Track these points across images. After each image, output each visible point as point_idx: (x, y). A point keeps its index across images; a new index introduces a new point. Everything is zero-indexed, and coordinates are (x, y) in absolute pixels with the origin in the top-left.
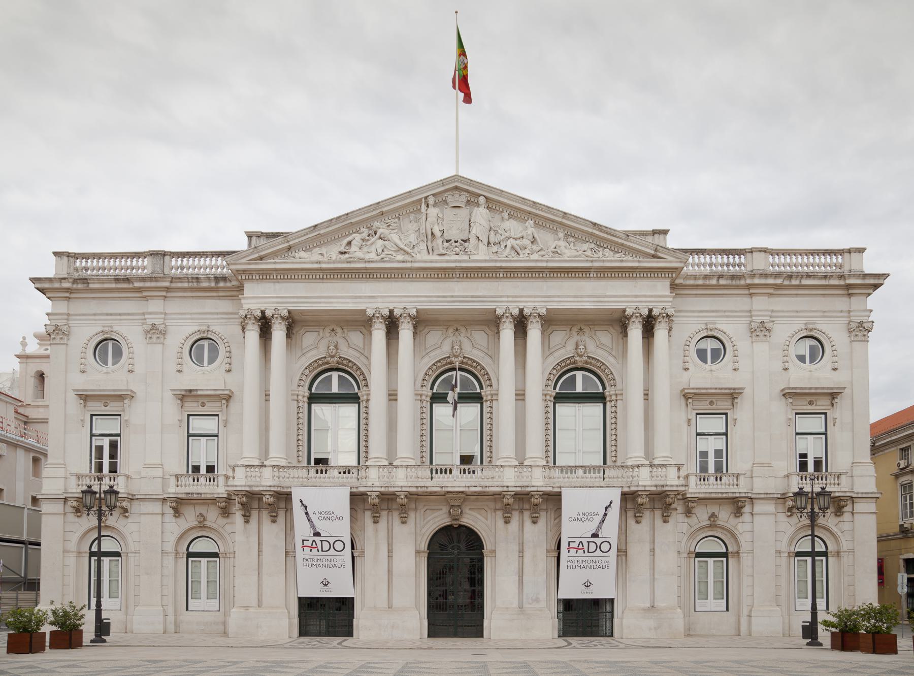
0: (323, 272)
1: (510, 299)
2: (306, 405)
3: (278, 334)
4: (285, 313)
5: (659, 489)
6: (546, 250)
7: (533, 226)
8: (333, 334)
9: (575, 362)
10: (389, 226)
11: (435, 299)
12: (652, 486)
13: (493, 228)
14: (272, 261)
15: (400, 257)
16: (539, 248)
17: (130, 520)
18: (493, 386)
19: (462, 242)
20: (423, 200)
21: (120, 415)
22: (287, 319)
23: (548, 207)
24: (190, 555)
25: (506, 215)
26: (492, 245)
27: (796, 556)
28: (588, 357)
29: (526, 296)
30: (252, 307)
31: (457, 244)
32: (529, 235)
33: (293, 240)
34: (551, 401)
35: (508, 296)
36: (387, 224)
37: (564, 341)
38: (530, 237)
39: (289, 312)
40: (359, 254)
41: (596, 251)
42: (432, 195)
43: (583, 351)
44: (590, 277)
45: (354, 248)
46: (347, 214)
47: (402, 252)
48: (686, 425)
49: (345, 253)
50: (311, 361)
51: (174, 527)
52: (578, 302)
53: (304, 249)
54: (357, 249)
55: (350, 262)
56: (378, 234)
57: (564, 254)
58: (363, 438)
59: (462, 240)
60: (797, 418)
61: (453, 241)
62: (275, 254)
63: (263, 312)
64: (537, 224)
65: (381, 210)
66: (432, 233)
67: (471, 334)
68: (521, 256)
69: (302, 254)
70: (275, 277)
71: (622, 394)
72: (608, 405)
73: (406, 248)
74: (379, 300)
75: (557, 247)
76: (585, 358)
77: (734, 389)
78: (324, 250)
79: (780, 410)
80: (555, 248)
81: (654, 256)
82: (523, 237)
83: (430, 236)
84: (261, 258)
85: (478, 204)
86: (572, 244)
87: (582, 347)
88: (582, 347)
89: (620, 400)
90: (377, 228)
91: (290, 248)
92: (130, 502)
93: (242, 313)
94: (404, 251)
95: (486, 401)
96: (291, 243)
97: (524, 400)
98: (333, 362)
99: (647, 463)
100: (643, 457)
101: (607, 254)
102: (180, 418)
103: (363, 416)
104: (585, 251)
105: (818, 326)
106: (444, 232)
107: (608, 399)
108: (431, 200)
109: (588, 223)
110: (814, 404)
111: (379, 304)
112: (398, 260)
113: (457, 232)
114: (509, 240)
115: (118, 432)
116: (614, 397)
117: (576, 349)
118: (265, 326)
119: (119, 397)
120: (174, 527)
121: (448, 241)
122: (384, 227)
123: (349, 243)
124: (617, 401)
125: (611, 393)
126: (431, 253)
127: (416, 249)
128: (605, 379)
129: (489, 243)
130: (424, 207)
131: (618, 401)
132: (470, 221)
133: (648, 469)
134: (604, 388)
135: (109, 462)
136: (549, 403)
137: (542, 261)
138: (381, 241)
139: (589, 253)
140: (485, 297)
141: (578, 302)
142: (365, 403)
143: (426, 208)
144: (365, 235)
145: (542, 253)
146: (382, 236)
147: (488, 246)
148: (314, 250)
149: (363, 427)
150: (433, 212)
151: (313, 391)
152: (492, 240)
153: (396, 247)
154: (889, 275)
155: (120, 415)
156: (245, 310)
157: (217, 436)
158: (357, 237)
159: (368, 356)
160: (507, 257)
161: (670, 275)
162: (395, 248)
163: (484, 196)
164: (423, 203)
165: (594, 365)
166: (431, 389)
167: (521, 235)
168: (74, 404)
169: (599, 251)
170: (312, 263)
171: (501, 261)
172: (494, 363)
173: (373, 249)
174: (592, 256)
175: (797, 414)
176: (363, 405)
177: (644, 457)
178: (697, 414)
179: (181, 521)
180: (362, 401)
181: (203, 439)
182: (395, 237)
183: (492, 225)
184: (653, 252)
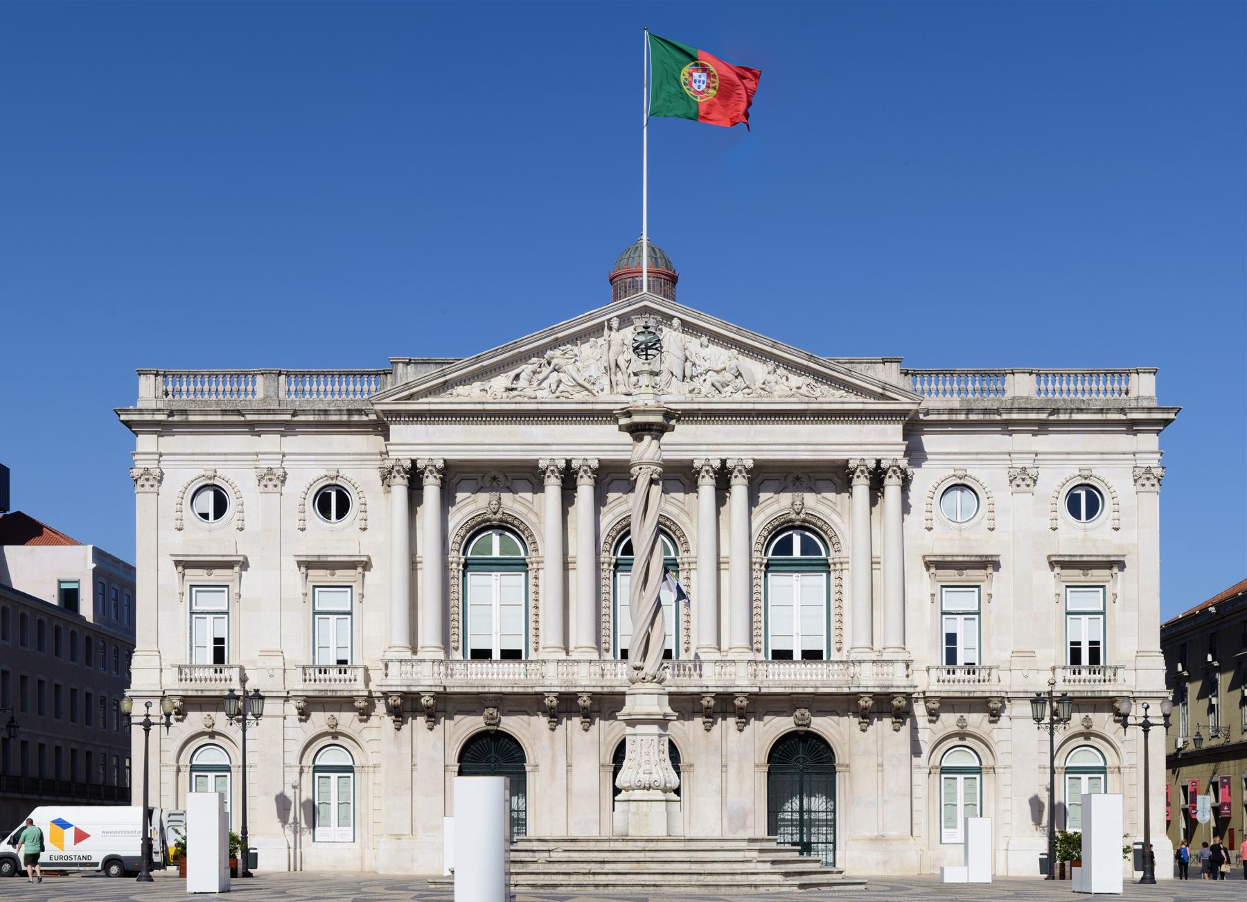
1: (711, 447)
4: (440, 464)
8: (495, 484)
9: (791, 521)
10: (564, 354)
11: (620, 448)
13: (689, 358)
15: (579, 396)
16: (744, 385)
18: (691, 550)
21: (227, 586)
26: (689, 380)
28: (807, 513)
32: (733, 369)
33: (450, 373)
34: (761, 571)
35: (708, 444)
39: (445, 461)
40: (529, 392)
43: (800, 507)
45: (522, 383)
47: (579, 388)
49: (512, 389)
50: (467, 519)
55: (520, 403)
56: (552, 365)
57: (775, 391)
58: (532, 618)
66: (617, 365)
69: (460, 390)
73: (585, 384)
74: (554, 448)
75: (766, 382)
76: (802, 516)
77: (987, 556)
78: (487, 385)
79: (1049, 581)
80: (764, 383)
82: (725, 369)
84: (410, 397)
86: (785, 378)
89: (845, 569)
90: (551, 358)
91: (445, 382)
94: (584, 387)
95: (683, 570)
96: (448, 377)
98: (495, 520)
102: (304, 592)
103: (532, 589)
105: (1094, 473)
107: (832, 567)
111: (554, 453)
112: (577, 400)
115: (225, 608)
116: (838, 566)
117: (792, 505)
118: (415, 478)
119: (229, 565)
123: (517, 377)
125: (835, 560)
129: (684, 376)
131: (844, 571)
135: (214, 647)
139: (804, 390)
140: (681, 444)
144: (536, 366)
145: (747, 390)
146: (557, 367)
147: (683, 381)
149: (532, 604)
151: (469, 555)
153: (571, 380)
155: (227, 586)
157: (350, 613)
159: (538, 512)
162: (572, 383)
165: (815, 525)
166: (614, 555)
168: (170, 573)
171: (699, 403)
172: (692, 522)
176: (532, 574)
180: (531, 570)
181: (333, 618)
182: (571, 368)
183: (688, 355)
184: (880, 391)
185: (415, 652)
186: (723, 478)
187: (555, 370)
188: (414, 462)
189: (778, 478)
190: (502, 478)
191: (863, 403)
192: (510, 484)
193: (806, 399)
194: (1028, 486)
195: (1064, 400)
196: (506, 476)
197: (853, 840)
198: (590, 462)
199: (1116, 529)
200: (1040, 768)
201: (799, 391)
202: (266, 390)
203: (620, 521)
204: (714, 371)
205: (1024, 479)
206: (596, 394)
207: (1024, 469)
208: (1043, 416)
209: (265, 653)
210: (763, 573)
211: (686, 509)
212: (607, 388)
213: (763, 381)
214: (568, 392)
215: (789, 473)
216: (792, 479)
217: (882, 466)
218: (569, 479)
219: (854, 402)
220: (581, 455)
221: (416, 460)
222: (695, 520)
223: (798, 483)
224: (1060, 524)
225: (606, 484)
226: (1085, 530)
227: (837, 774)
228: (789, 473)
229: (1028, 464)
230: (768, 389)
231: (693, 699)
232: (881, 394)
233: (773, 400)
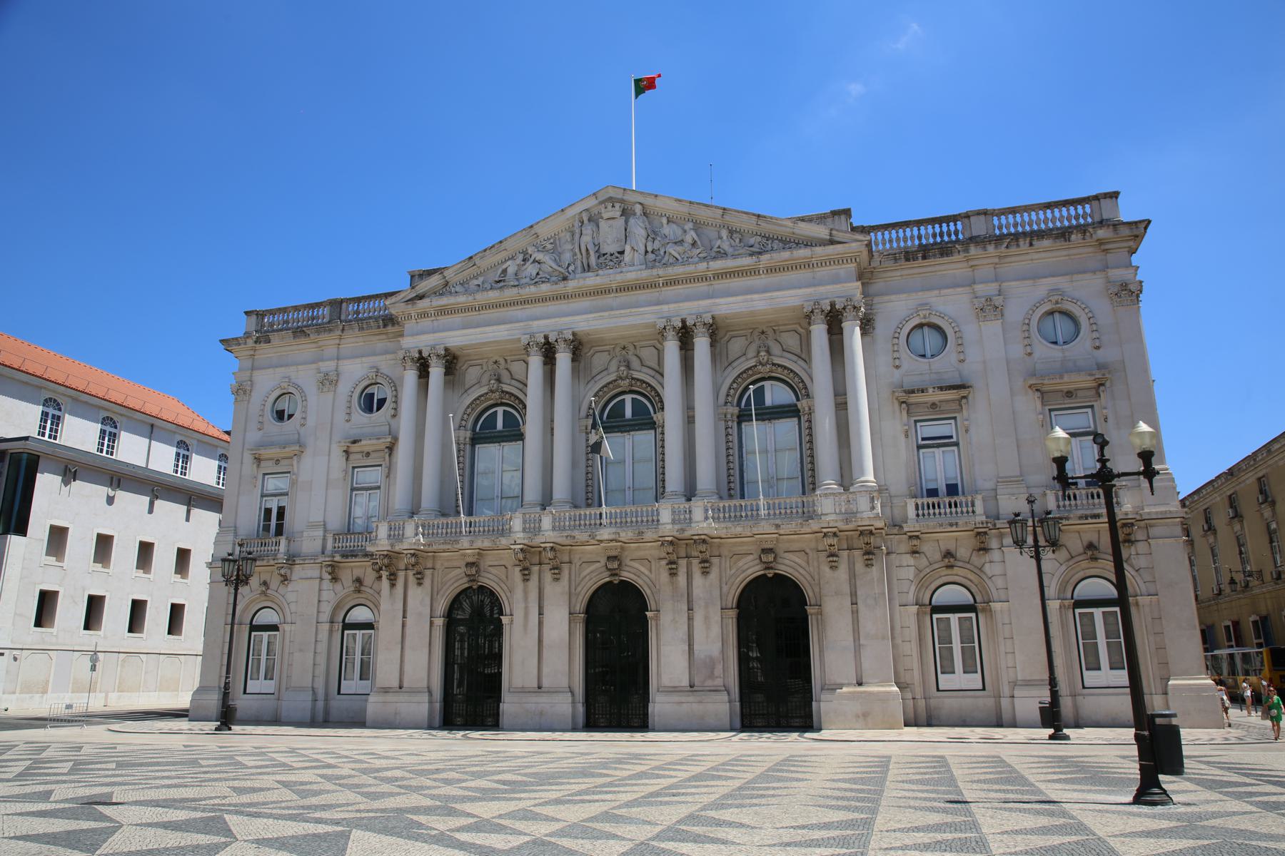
2: (468, 447)
3: (436, 372)
17: (290, 588)
22: (445, 356)
24: (347, 626)
25: (664, 220)
31: (614, 256)
34: (733, 421)
48: (903, 436)
49: (500, 281)
51: (331, 594)
56: (533, 258)
59: (619, 253)
63: (420, 352)
66: (587, 250)
81: (832, 242)
86: (737, 240)
87: (763, 354)
88: (763, 354)
92: (290, 568)
93: (401, 354)
120: (331, 594)
121: (604, 255)
123: (505, 271)
127: (571, 268)
129: (646, 252)
132: (626, 230)
136: (730, 423)
152: (649, 249)
154: (1149, 222)
163: (640, 203)
167: (680, 239)
178: (916, 422)
179: (338, 587)
186: (685, 336)
196: (506, 360)
197: (828, 689)
199: (1098, 348)
201: (751, 249)
202: (331, 315)
205: (990, 308)
207: (989, 299)
209: (312, 526)
210: (735, 424)
211: (661, 371)
212: (579, 269)
213: (717, 246)
215: (754, 329)
216: (757, 334)
217: (837, 307)
218: (549, 353)
223: (763, 336)
227: (809, 617)
230: (722, 251)
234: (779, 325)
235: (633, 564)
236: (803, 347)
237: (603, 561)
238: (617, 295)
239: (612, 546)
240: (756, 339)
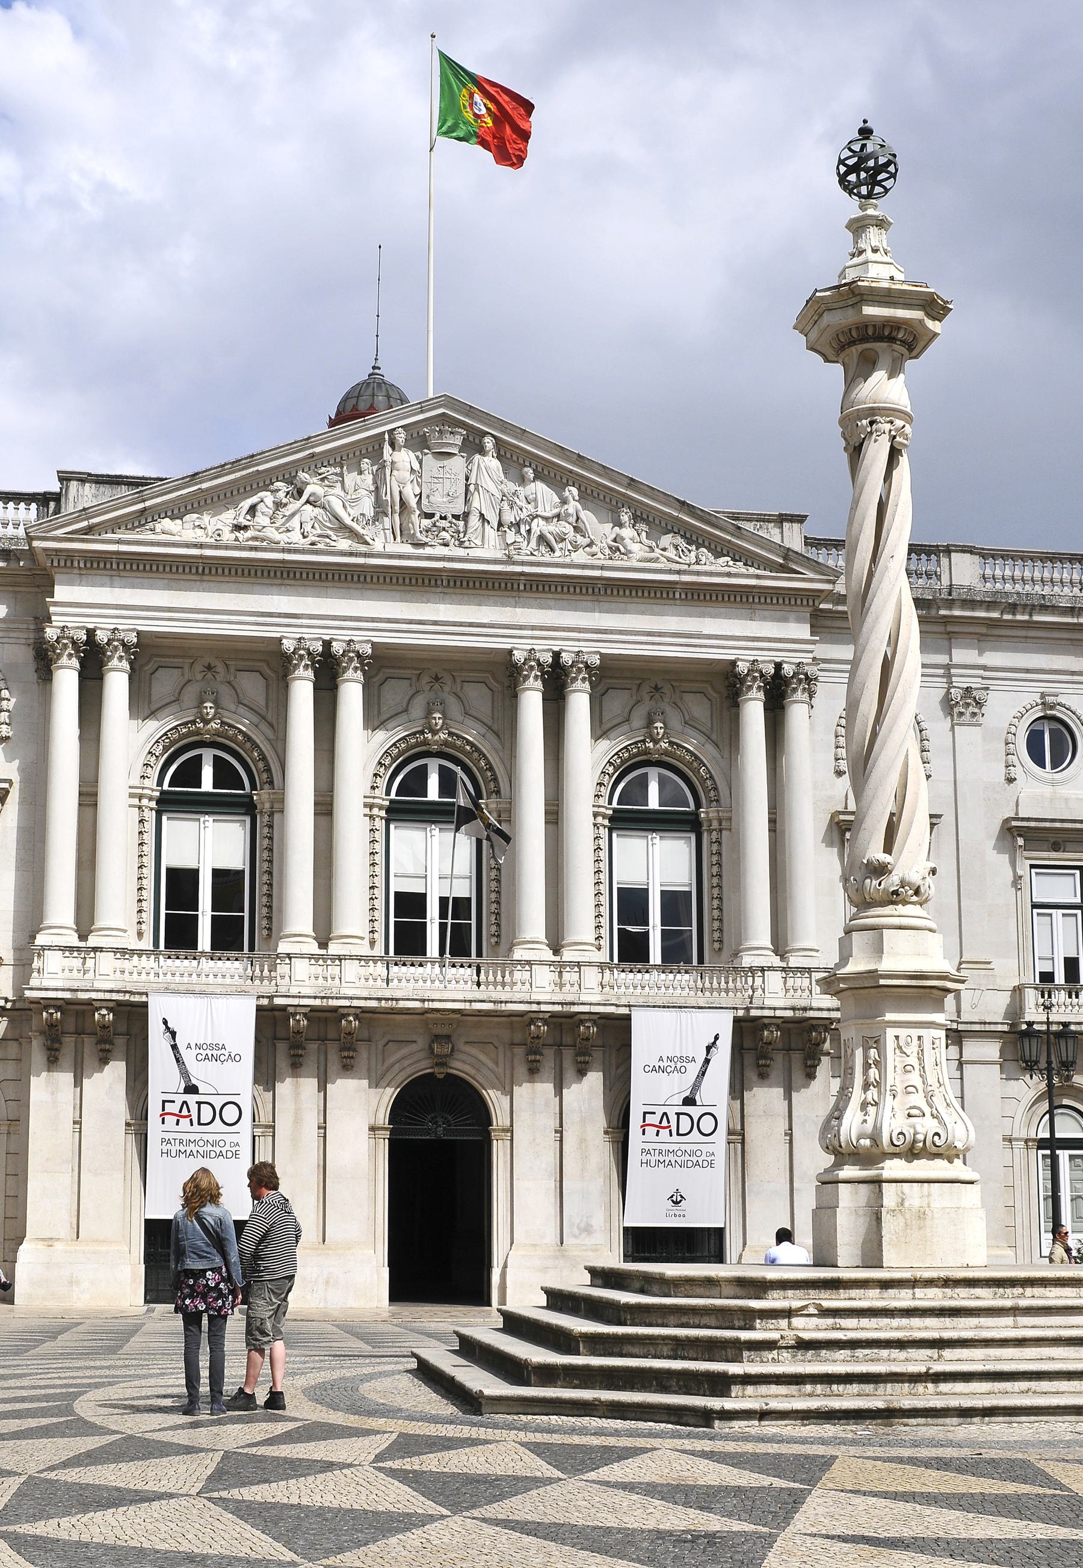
0: (204, 561)
5: (799, 1014)
6: (600, 544)
7: (577, 498)
10: (322, 480)
12: (785, 1009)
14: (110, 536)
15: (344, 544)
16: (587, 541)
19: (454, 520)
20: (387, 436)
23: (604, 467)
25: (530, 473)
27: (1039, 1148)
29: (564, 629)
30: (71, 622)
33: (152, 498)
36: (320, 474)
37: (627, 710)
38: (573, 519)
40: (272, 533)
41: (685, 549)
42: (401, 427)
44: (674, 598)
46: (253, 456)
49: (245, 528)
52: (653, 644)
53: (169, 514)
54: (265, 521)
59: (454, 516)
60: (1033, 874)
61: (437, 517)
62: (115, 525)
64: (582, 492)
65: (311, 451)
66: (403, 503)
67: (462, 688)
68: (558, 553)
69: (166, 523)
70: (115, 566)
71: (730, 819)
72: (705, 836)
73: (354, 525)
75: (618, 539)
80: (615, 540)
81: (783, 568)
83: (397, 508)
85: (482, 451)
89: (726, 829)
96: (148, 504)
97: (557, 823)
99: (776, 961)
100: (768, 949)
101: (703, 559)
104: (664, 549)
106: (421, 497)
108: (401, 437)
109: (671, 499)
110: (1062, 849)
113: (445, 500)
114: (536, 520)
121: (430, 516)
122: (315, 481)
123: (252, 510)
124: (721, 830)
126: (398, 538)
128: (700, 788)
130: (387, 448)
132: (467, 479)
133: (779, 975)
134: (698, 805)
137: (593, 567)
138: (308, 507)
139: (671, 553)
141: (653, 644)
142: (266, 818)
143: (391, 452)
144: (281, 495)
147: (498, 530)
148: (187, 518)
150: (405, 458)
156: (58, 627)
158: (268, 498)
160: (532, 554)
161: (811, 603)
164: (387, 443)
169: (690, 551)
170: (188, 545)
173: (295, 522)
174: (677, 558)
175: (1032, 866)
177: (771, 947)
185: (83, 937)
187: (308, 502)
188: (91, 633)
189: (628, 686)
190: (220, 668)
191: (758, 577)
192: (232, 678)
193: (677, 567)
194: (974, 714)
195: (1018, 593)
198: (358, 647)
200: (1004, 1140)
203: (397, 741)
204: (543, 518)
206: (371, 542)
207: (968, 690)
208: (995, 615)
214: (328, 537)
219: (744, 576)
220: (347, 635)
221: (94, 630)
222: (508, 745)
223: (657, 695)
224: (1017, 772)
225: (377, 684)
226: (1053, 783)
228: (644, 680)
229: (976, 682)
230: (622, 550)
231: (512, 1023)
232: (781, 565)
233: (628, 564)
234: (681, 681)
235: (468, 1048)
236: (715, 723)
237: (422, 1042)
238: (446, 590)
239: (437, 1019)
240: (647, 697)
